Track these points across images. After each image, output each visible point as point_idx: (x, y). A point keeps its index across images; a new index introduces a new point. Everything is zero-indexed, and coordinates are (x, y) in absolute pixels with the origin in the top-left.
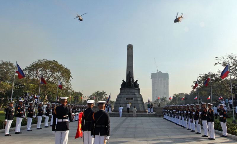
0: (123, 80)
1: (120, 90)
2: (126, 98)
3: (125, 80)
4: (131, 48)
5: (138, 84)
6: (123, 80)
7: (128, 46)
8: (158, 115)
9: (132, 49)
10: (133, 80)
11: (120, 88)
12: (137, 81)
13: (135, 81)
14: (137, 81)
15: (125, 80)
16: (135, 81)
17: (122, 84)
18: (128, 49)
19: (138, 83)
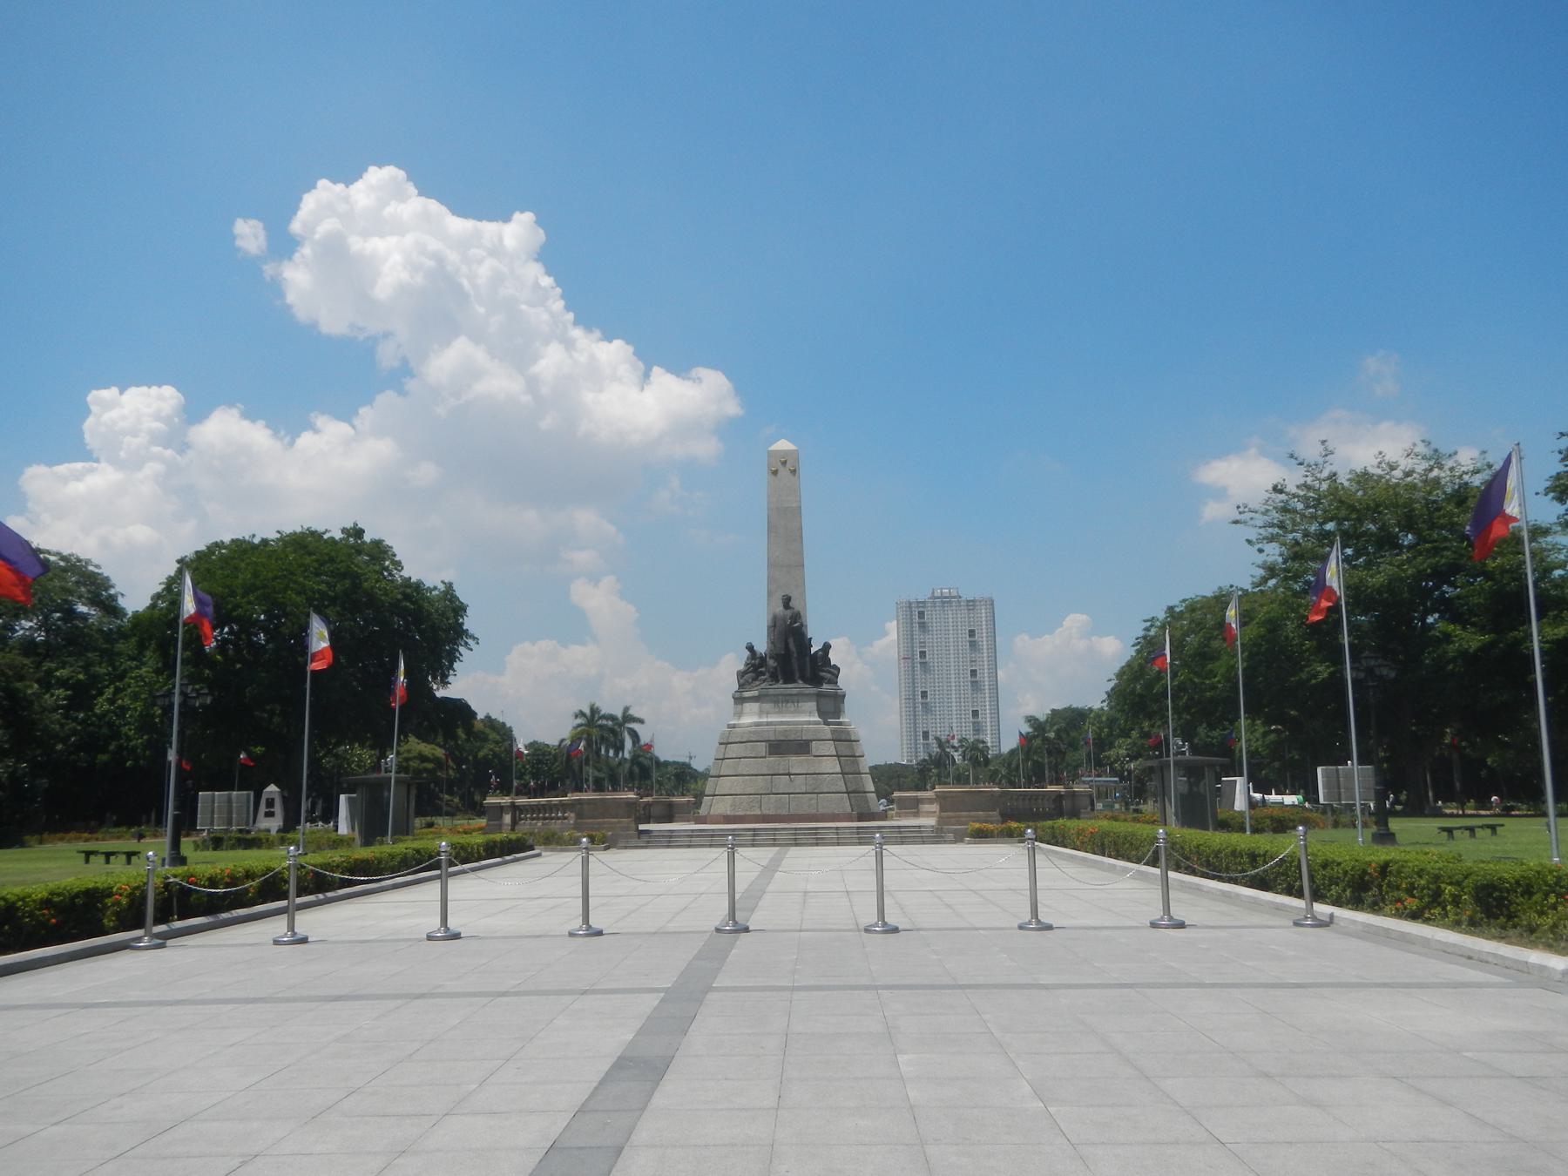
0: (750, 648)
3: (762, 647)
4: (789, 465)
6: (750, 648)
12: (827, 647)
15: (762, 647)
17: (742, 667)
19: (834, 658)
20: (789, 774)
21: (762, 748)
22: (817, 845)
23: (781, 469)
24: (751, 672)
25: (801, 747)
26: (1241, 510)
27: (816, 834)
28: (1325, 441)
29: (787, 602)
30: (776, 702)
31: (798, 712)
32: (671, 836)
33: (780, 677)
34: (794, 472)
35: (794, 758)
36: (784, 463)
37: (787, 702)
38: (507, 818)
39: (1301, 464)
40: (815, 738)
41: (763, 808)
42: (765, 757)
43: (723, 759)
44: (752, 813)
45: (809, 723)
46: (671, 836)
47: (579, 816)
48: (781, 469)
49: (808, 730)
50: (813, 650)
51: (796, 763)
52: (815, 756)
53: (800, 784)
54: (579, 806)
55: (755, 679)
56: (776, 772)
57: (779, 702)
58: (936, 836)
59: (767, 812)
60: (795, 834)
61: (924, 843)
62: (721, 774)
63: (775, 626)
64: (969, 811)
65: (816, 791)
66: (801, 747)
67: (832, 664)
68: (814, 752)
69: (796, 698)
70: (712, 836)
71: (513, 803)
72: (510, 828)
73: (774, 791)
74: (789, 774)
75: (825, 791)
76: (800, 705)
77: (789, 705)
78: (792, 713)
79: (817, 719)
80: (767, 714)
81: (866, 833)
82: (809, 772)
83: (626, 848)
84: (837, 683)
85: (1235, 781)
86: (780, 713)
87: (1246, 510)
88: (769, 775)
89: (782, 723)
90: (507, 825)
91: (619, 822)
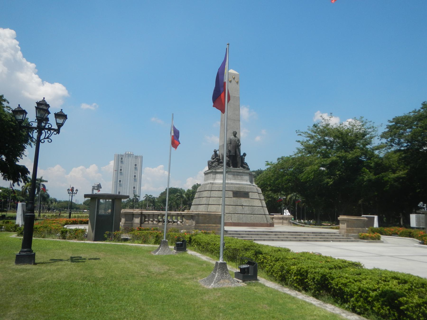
12: (245, 155)
14: (245, 155)
20: (242, 206)
21: (231, 194)
23: (233, 80)
24: (217, 162)
25: (245, 195)
26: (297, 132)
28: (332, 113)
29: (235, 134)
30: (234, 175)
31: (242, 180)
33: (231, 165)
34: (237, 83)
35: (243, 199)
36: (234, 78)
37: (238, 175)
38: (137, 221)
39: (323, 119)
40: (251, 191)
41: (233, 220)
42: (232, 198)
43: (210, 197)
44: (229, 222)
45: (247, 185)
47: (197, 223)
48: (233, 80)
49: (248, 188)
51: (244, 201)
52: (251, 199)
53: (247, 210)
54: (197, 217)
55: (218, 165)
56: (237, 204)
57: (235, 175)
58: (347, 239)
59: (234, 221)
61: (340, 241)
62: (209, 204)
63: (230, 143)
64: (356, 227)
65: (253, 213)
66: (245, 195)
68: (250, 197)
69: (241, 174)
71: (141, 213)
72: (139, 225)
73: (236, 212)
74: (242, 206)
75: (256, 213)
76: (243, 177)
77: (239, 176)
78: (239, 180)
79: (249, 183)
80: (230, 179)
82: (250, 205)
85: (374, 217)
86: (235, 179)
87: (299, 132)
88: (234, 205)
89: (237, 184)
90: (138, 224)
91: (217, 226)
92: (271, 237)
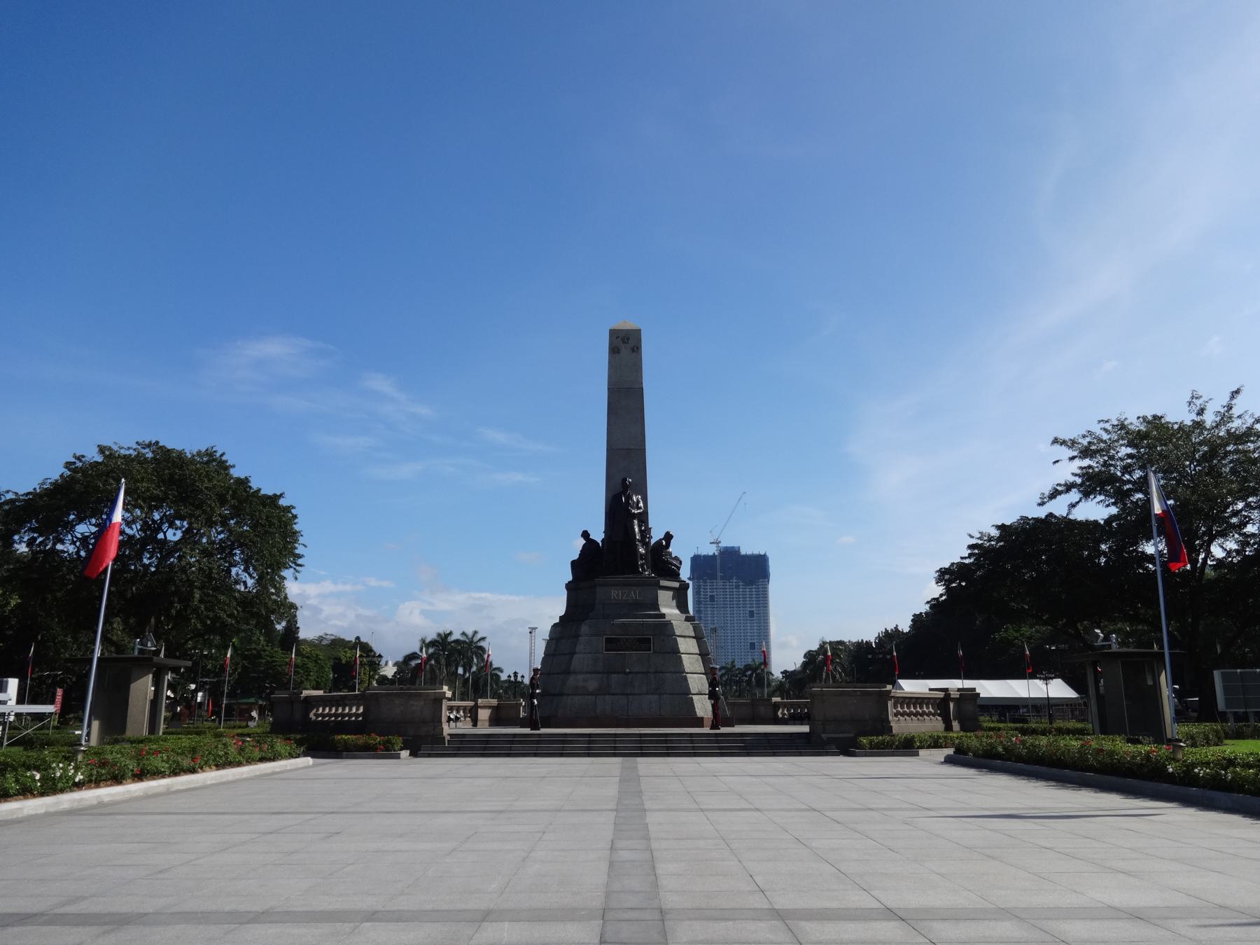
0: (585, 535)
1: (565, 592)
2: (608, 641)
3: (598, 535)
5: (676, 558)
6: (585, 535)
7: (610, 330)
8: (830, 741)
9: (637, 349)
10: (646, 532)
11: (570, 578)
12: (668, 537)
13: (656, 535)
14: (668, 537)
16: (656, 535)
17: (576, 557)
18: (614, 350)
22: (668, 755)
27: (666, 741)
32: (487, 742)
46: (487, 742)
50: (653, 541)
60: (641, 742)
67: (673, 556)
70: (538, 742)
81: (728, 742)
83: (429, 756)
84: (679, 575)
92: (565, 749)
